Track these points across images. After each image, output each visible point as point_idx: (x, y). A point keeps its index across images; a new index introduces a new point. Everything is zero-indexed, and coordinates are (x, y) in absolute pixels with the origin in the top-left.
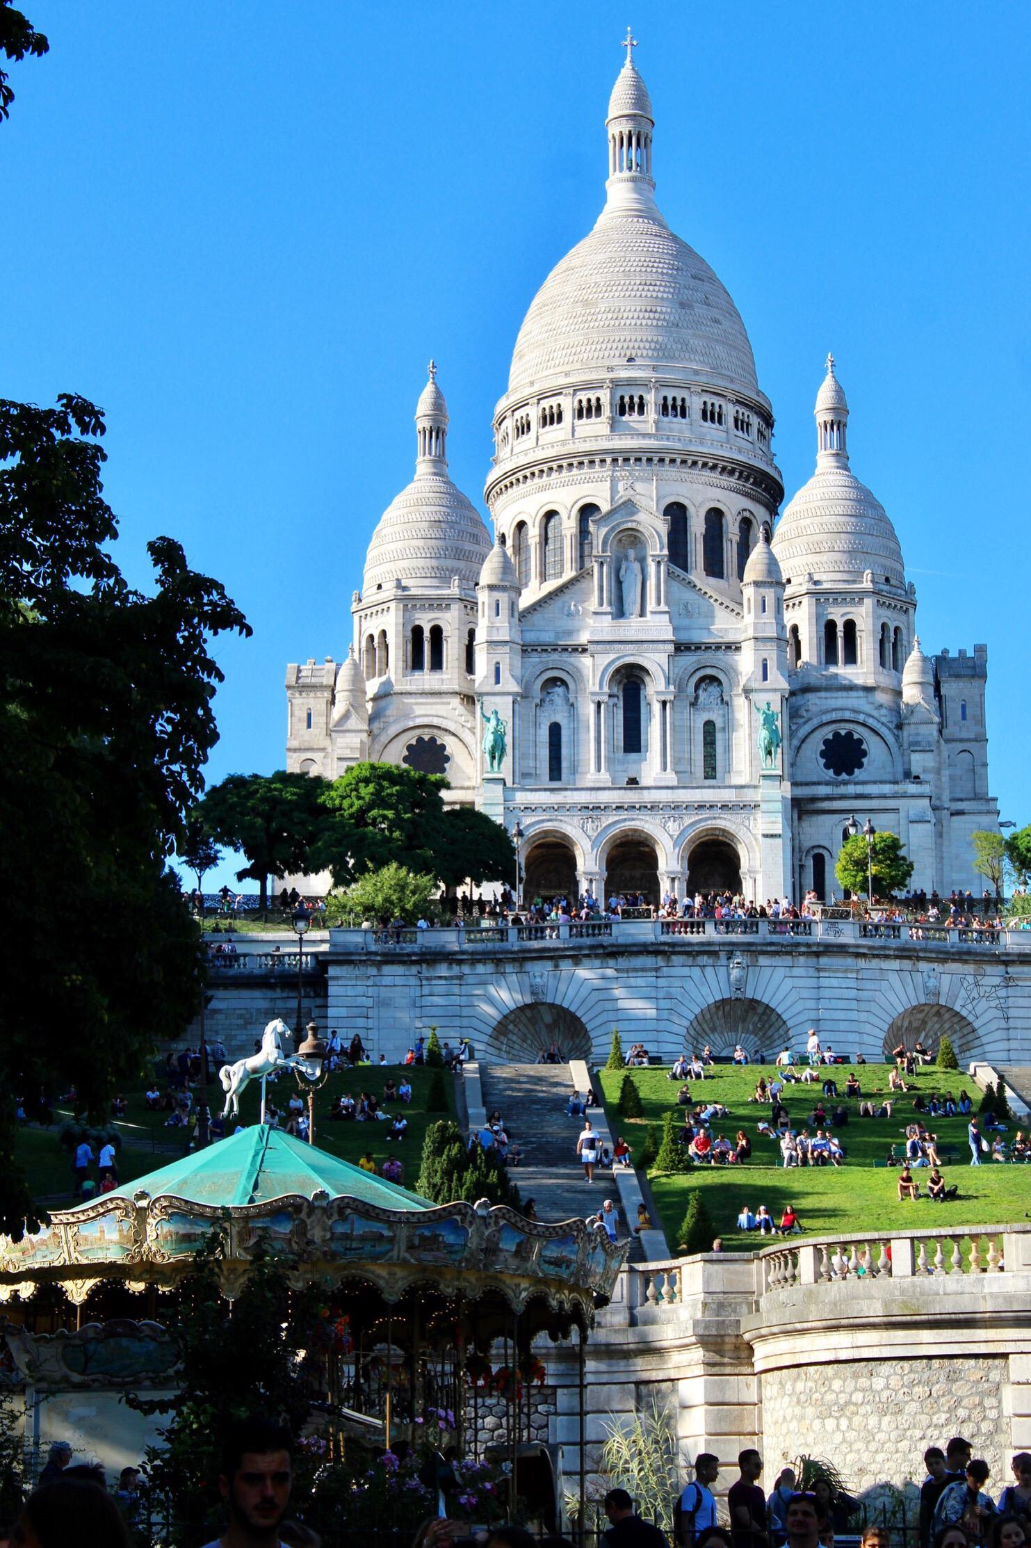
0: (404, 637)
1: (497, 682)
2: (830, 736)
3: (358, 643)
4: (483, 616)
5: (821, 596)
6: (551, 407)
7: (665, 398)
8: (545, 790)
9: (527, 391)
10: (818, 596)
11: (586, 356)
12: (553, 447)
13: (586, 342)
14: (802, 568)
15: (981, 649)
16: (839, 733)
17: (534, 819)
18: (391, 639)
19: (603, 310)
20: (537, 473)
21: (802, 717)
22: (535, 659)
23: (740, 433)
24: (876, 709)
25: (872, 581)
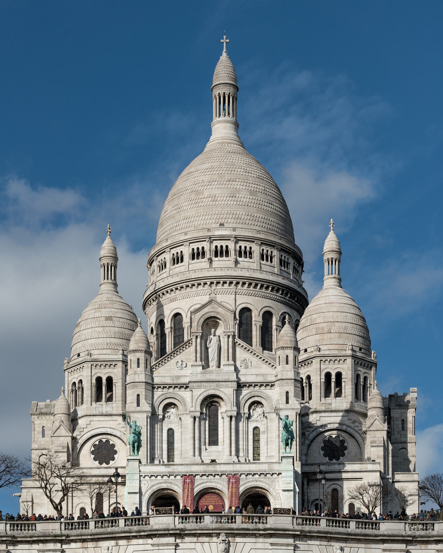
1: (138, 405)
4: (131, 368)
6: (177, 253)
12: (178, 276)
20: (169, 290)
23: (283, 268)
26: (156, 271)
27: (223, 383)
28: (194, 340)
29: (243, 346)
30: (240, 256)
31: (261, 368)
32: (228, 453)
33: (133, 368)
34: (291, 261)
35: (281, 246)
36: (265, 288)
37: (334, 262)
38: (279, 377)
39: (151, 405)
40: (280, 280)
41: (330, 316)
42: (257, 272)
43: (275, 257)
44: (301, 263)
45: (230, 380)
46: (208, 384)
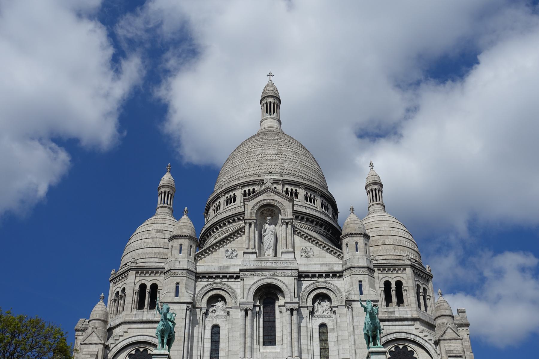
0: (134, 290)
1: (177, 295)
2: (393, 349)
3: (111, 296)
4: (171, 255)
5: (382, 267)
6: (231, 196)
7: (287, 189)
11: (248, 173)
13: (248, 167)
19: (257, 154)
23: (324, 210)
24: (421, 332)
25: (410, 260)
28: (247, 227)
29: (303, 235)
31: (325, 257)
33: (174, 254)
34: (330, 207)
35: (322, 193)
36: (310, 222)
37: (377, 192)
38: (349, 265)
39: (192, 296)
40: (323, 216)
41: (383, 231)
42: (303, 208)
43: (317, 201)
44: (337, 213)
46: (263, 272)
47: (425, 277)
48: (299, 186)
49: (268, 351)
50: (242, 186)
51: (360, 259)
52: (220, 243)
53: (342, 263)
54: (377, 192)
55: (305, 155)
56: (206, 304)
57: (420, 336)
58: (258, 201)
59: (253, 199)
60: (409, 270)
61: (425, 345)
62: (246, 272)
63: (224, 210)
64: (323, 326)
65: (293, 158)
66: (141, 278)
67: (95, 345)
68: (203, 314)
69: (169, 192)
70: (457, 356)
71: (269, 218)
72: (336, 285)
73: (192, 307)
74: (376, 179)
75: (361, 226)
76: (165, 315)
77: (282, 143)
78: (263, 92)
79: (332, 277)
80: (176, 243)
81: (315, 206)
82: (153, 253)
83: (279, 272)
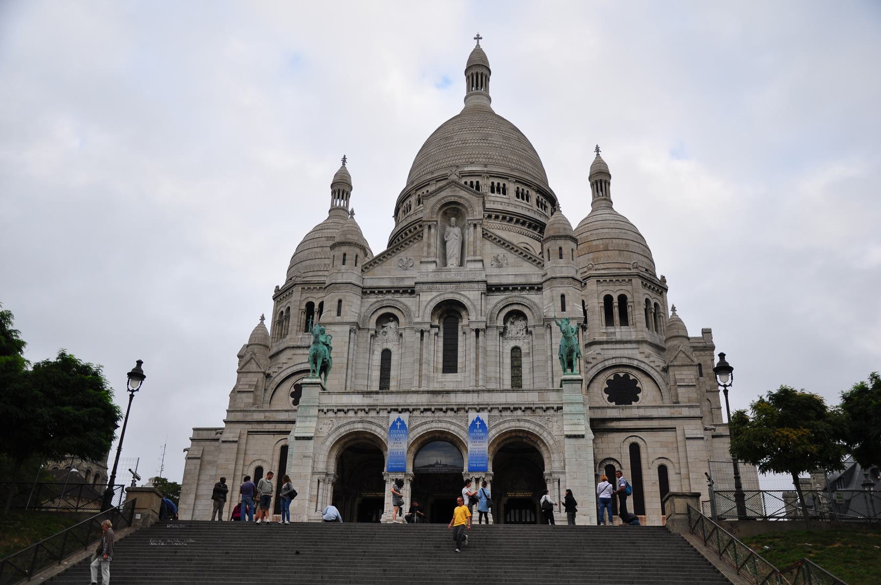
1: (339, 314)
2: (612, 378)
7: (493, 183)
8: (358, 393)
9: (410, 188)
10: (599, 279)
11: (445, 164)
12: (422, 212)
14: (585, 263)
15: (707, 332)
16: (618, 375)
17: (345, 421)
18: (292, 311)
19: (456, 140)
21: (591, 363)
22: (372, 299)
23: (540, 209)
24: (646, 357)
25: (637, 268)
26: (401, 216)
27: (466, 285)
29: (495, 239)
30: (493, 192)
31: (522, 266)
32: (473, 383)
33: (336, 265)
34: (548, 205)
36: (521, 224)
38: (549, 276)
39: (357, 315)
45: (476, 280)
46: (443, 286)
47: (658, 290)
48: (508, 179)
49: (448, 380)
50: (437, 181)
51: (564, 268)
52: (392, 250)
53: (542, 272)
54: (603, 184)
55: (519, 140)
56: (375, 325)
57: (646, 362)
58: (440, 198)
59: (433, 196)
60: (637, 282)
61: (651, 372)
62: (422, 286)
63: (416, 211)
64: (516, 350)
65: (501, 144)
66: (308, 295)
67: (253, 374)
68: (371, 336)
69: (344, 190)
70: (688, 386)
71: (453, 219)
72: (533, 300)
73: (357, 328)
74: (602, 168)
75: (567, 227)
76: (317, 337)
77: (488, 125)
78: (469, 60)
79: (528, 290)
80: (339, 252)
81: (528, 203)
82: (323, 265)
83: (462, 285)
